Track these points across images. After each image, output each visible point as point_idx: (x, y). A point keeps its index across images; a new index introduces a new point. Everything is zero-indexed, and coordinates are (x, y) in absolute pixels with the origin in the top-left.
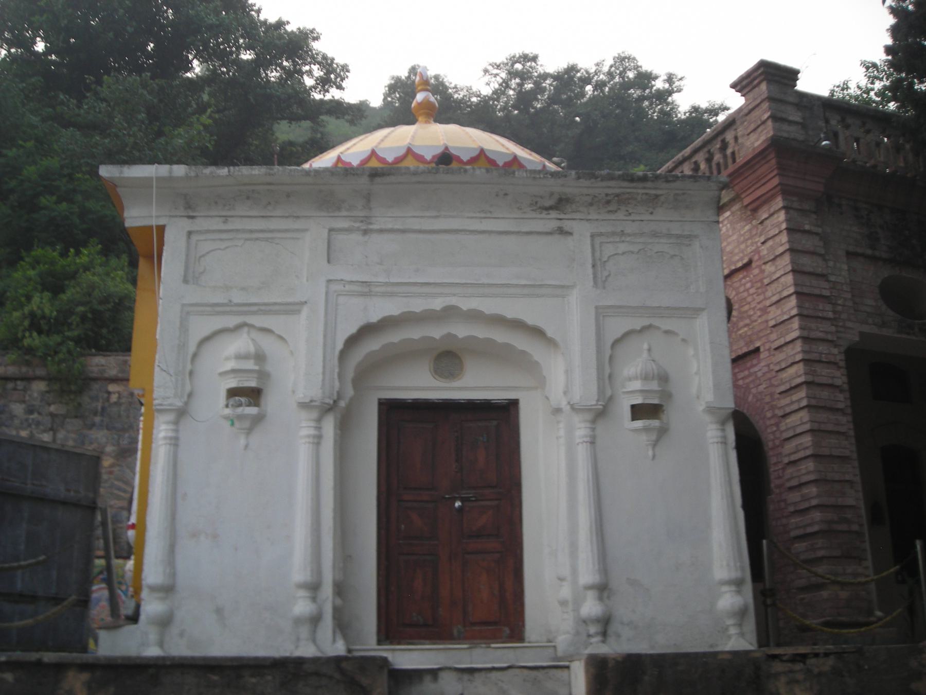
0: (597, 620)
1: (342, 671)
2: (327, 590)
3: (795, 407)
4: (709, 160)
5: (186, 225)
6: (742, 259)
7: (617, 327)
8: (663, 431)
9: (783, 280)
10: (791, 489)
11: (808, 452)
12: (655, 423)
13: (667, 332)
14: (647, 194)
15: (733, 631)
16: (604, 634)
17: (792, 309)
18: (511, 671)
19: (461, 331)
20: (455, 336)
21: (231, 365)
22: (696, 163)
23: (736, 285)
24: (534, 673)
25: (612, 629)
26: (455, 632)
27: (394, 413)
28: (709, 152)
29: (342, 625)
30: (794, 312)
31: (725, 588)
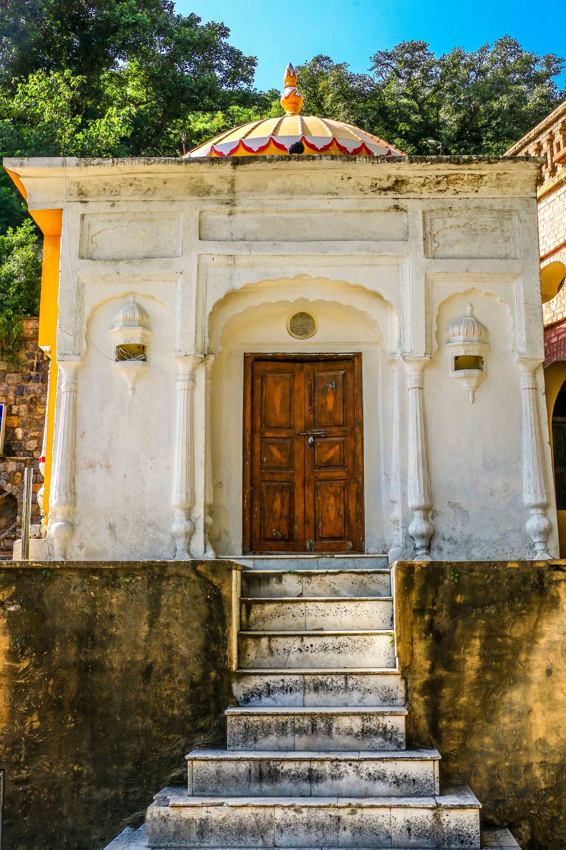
0: (422, 536)
1: (198, 573)
2: (199, 511)
4: (551, 141)
5: (80, 208)
14: (472, 175)
15: (539, 547)
16: (429, 548)
20: (307, 300)
22: (539, 143)
24: (361, 577)
25: (435, 544)
26: (308, 546)
28: (551, 133)
29: (213, 538)
31: (533, 511)
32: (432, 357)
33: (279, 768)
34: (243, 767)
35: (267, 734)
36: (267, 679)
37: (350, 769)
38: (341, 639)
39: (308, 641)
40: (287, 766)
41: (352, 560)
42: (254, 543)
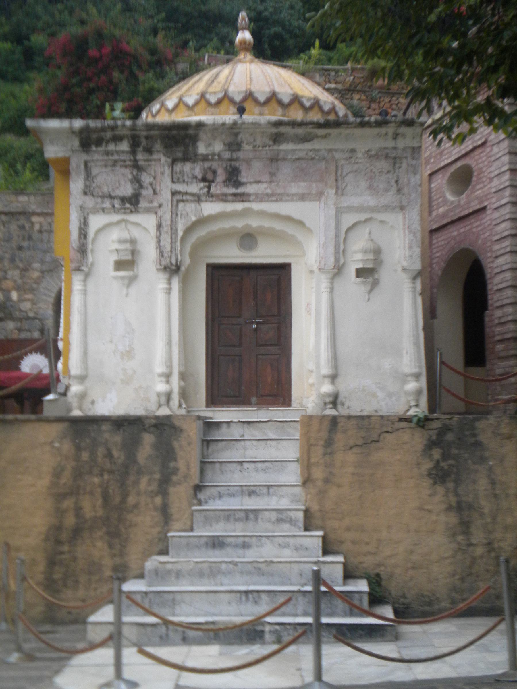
3: (502, 251)
5: (85, 157)
6: (479, 139)
7: (348, 220)
8: (375, 284)
9: (503, 158)
10: (498, 307)
11: (509, 284)
12: (370, 280)
13: (382, 222)
17: (505, 181)
18: (270, 423)
19: (254, 223)
21: (117, 246)
23: (477, 157)
25: (339, 401)
27: (217, 272)
30: (507, 184)
31: (409, 378)
32: (338, 270)
33: (225, 541)
34: (203, 540)
35: (218, 521)
36: (219, 489)
37: (268, 542)
38: (267, 464)
39: (246, 465)
40: (229, 540)
41: (280, 411)
42: (214, 399)
